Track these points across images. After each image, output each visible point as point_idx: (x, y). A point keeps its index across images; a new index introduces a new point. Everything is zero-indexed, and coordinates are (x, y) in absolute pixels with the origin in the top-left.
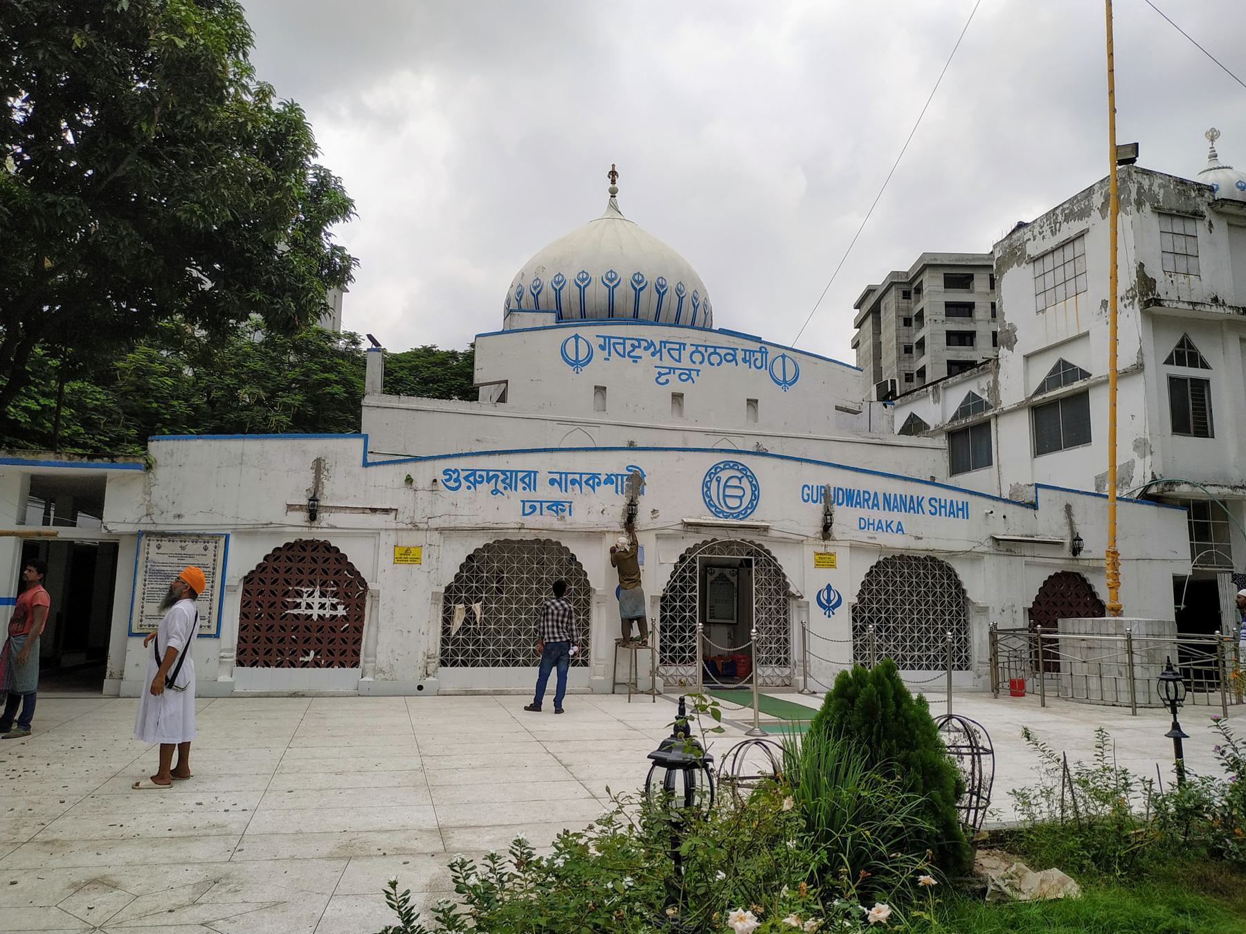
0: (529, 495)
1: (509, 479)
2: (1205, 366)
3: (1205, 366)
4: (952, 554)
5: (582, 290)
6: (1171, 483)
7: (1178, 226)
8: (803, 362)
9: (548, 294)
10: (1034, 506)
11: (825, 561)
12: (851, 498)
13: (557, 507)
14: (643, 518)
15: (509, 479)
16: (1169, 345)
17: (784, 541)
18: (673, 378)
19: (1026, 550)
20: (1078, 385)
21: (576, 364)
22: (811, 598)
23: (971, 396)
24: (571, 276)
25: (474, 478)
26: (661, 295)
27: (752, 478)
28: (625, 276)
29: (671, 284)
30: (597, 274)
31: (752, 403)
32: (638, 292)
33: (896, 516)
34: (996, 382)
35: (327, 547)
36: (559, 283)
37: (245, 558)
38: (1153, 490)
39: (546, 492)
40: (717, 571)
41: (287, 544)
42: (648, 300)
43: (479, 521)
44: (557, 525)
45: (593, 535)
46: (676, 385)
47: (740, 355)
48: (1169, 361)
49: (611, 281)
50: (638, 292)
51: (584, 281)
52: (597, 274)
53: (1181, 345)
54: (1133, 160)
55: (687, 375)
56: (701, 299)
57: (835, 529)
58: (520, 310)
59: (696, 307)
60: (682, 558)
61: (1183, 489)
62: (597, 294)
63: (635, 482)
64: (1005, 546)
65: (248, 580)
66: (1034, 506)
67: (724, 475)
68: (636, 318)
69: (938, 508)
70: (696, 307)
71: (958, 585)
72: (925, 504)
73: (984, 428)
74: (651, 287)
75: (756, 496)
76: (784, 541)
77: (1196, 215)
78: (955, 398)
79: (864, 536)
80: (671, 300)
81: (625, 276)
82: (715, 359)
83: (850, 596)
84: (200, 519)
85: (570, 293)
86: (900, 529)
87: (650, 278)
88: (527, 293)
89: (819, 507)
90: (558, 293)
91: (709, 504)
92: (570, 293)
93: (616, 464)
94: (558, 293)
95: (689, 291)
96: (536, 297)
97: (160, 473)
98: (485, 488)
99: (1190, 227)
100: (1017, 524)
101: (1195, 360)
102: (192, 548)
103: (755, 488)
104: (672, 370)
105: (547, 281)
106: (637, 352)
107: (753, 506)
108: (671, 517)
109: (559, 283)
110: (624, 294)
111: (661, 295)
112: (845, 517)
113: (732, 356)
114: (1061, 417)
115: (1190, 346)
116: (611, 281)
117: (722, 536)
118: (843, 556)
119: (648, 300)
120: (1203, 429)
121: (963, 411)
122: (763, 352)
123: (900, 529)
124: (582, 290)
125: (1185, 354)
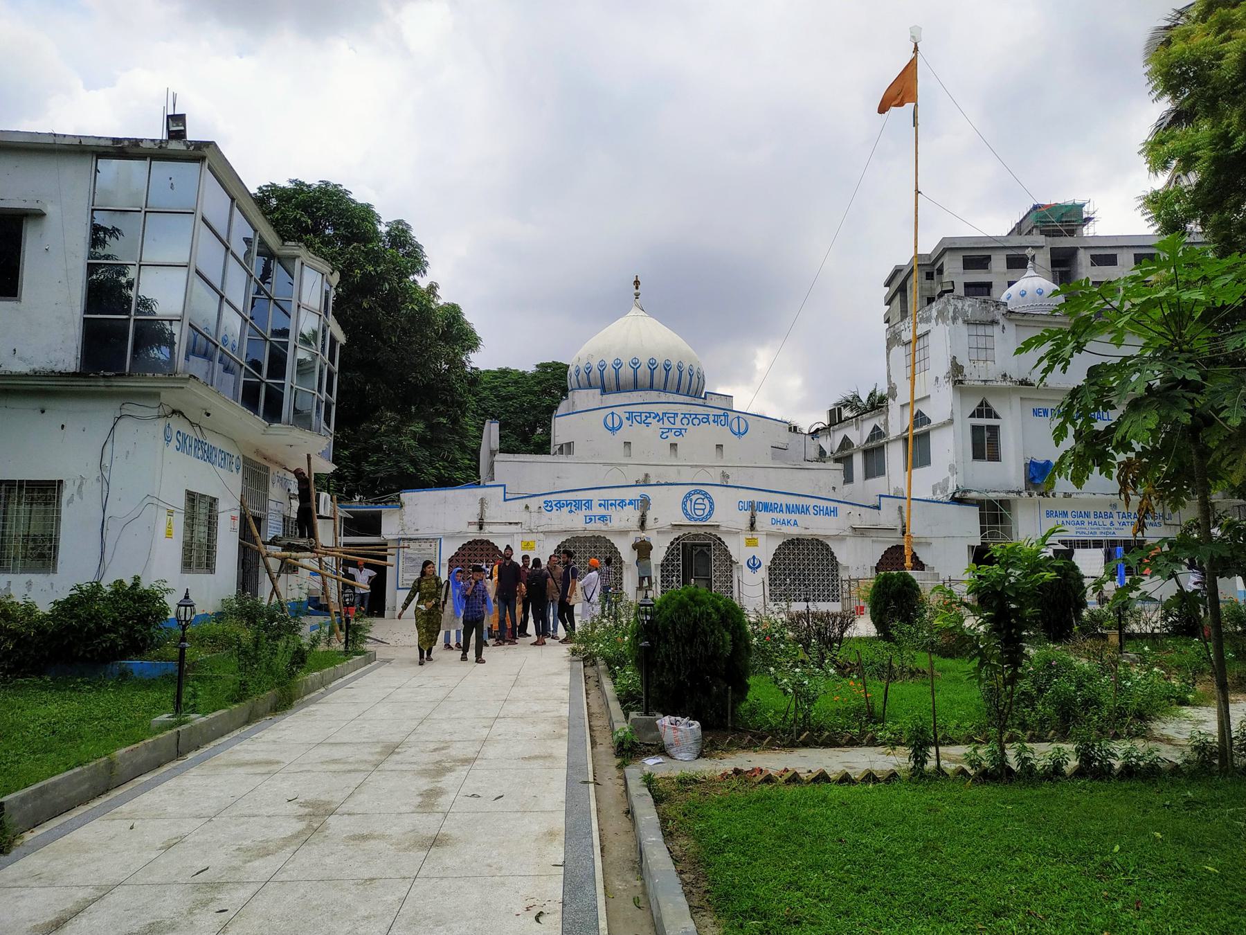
0: (588, 512)
1: (578, 505)
2: (997, 417)
3: (997, 417)
4: (828, 537)
5: (617, 371)
6: (965, 491)
7: (981, 330)
8: (750, 420)
9: (595, 372)
10: (878, 508)
11: (751, 542)
12: (766, 507)
13: (603, 518)
14: (650, 523)
15: (578, 505)
16: (973, 405)
17: (728, 533)
18: (671, 434)
19: (873, 533)
20: (924, 428)
21: (613, 430)
22: (743, 563)
23: (876, 428)
24: (609, 362)
25: (560, 505)
26: (667, 371)
27: (710, 499)
28: (644, 361)
29: (674, 363)
30: (626, 361)
31: (719, 447)
32: (652, 370)
33: (793, 517)
34: (887, 420)
35: (488, 542)
36: (602, 366)
37: (450, 549)
38: (957, 496)
39: (597, 511)
40: (699, 549)
41: (469, 543)
42: (659, 375)
43: (563, 527)
44: (604, 528)
45: (624, 533)
46: (672, 438)
47: (711, 418)
48: (972, 416)
49: (635, 364)
50: (652, 370)
51: (618, 365)
52: (626, 361)
53: (981, 405)
54: (952, 291)
55: (680, 432)
56: (695, 370)
57: (757, 524)
58: (580, 388)
59: (691, 376)
60: (672, 543)
61: (973, 495)
62: (626, 373)
63: (645, 503)
64: (859, 532)
65: (450, 560)
66: (878, 508)
67: (694, 498)
68: (651, 388)
69: (818, 511)
70: (691, 376)
71: (832, 554)
72: (811, 509)
73: (881, 448)
74: (661, 367)
75: (712, 509)
76: (728, 533)
77: (994, 322)
78: (867, 428)
79: (774, 528)
80: (674, 373)
81: (644, 361)
82: (696, 421)
83: (766, 560)
84: (428, 531)
85: (609, 372)
86: (795, 523)
87: (660, 361)
88: (582, 371)
89: (749, 512)
90: (602, 372)
91: (686, 514)
92: (609, 372)
93: (635, 493)
94: (602, 372)
95: (686, 366)
96: (588, 374)
97: (406, 508)
98: (565, 510)
99: (989, 330)
100: (868, 518)
101: (990, 413)
102: (424, 545)
103: (712, 504)
104: (670, 430)
105: (595, 364)
106: (649, 420)
107: (710, 514)
108: (665, 522)
109: (602, 366)
110: (643, 371)
111: (667, 371)
112: (763, 518)
113: (706, 419)
114: (918, 448)
115: (987, 405)
116: (635, 364)
117: (694, 531)
118: (762, 540)
119: (659, 375)
120: (995, 457)
121: (872, 438)
122: (726, 416)
123: (795, 523)
124: (617, 371)
125: (984, 410)
